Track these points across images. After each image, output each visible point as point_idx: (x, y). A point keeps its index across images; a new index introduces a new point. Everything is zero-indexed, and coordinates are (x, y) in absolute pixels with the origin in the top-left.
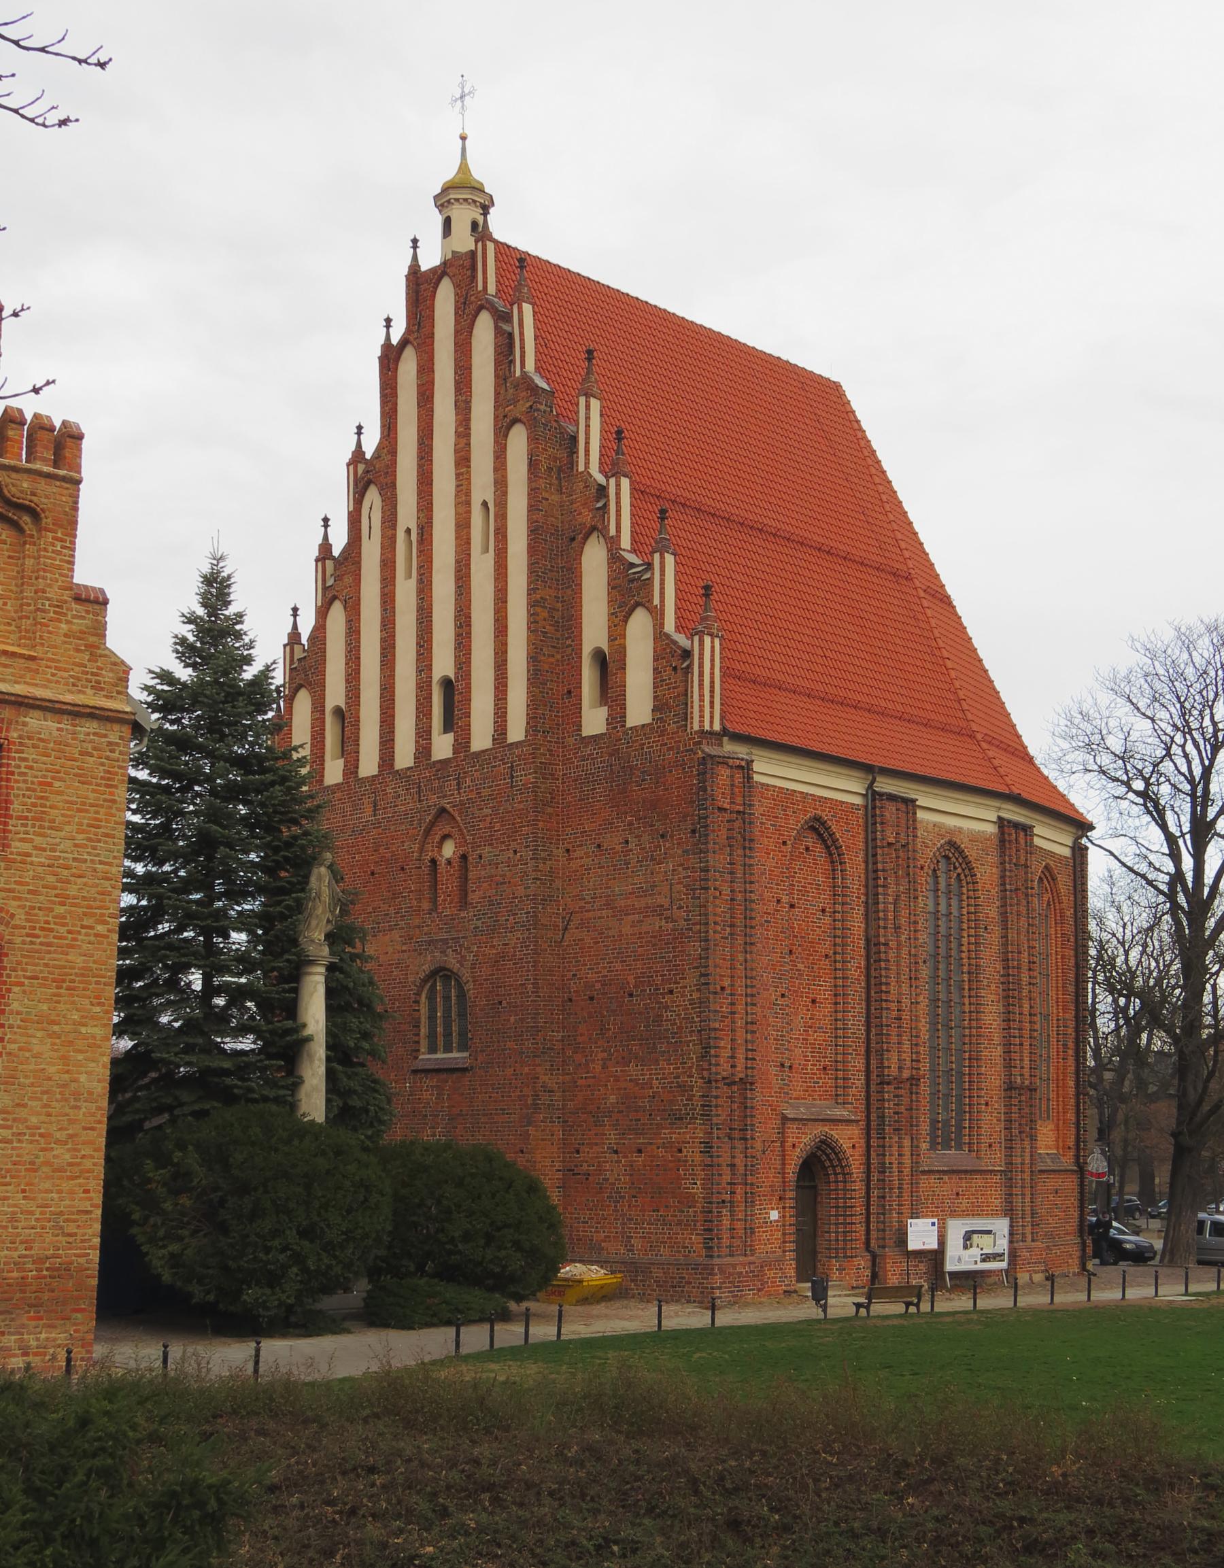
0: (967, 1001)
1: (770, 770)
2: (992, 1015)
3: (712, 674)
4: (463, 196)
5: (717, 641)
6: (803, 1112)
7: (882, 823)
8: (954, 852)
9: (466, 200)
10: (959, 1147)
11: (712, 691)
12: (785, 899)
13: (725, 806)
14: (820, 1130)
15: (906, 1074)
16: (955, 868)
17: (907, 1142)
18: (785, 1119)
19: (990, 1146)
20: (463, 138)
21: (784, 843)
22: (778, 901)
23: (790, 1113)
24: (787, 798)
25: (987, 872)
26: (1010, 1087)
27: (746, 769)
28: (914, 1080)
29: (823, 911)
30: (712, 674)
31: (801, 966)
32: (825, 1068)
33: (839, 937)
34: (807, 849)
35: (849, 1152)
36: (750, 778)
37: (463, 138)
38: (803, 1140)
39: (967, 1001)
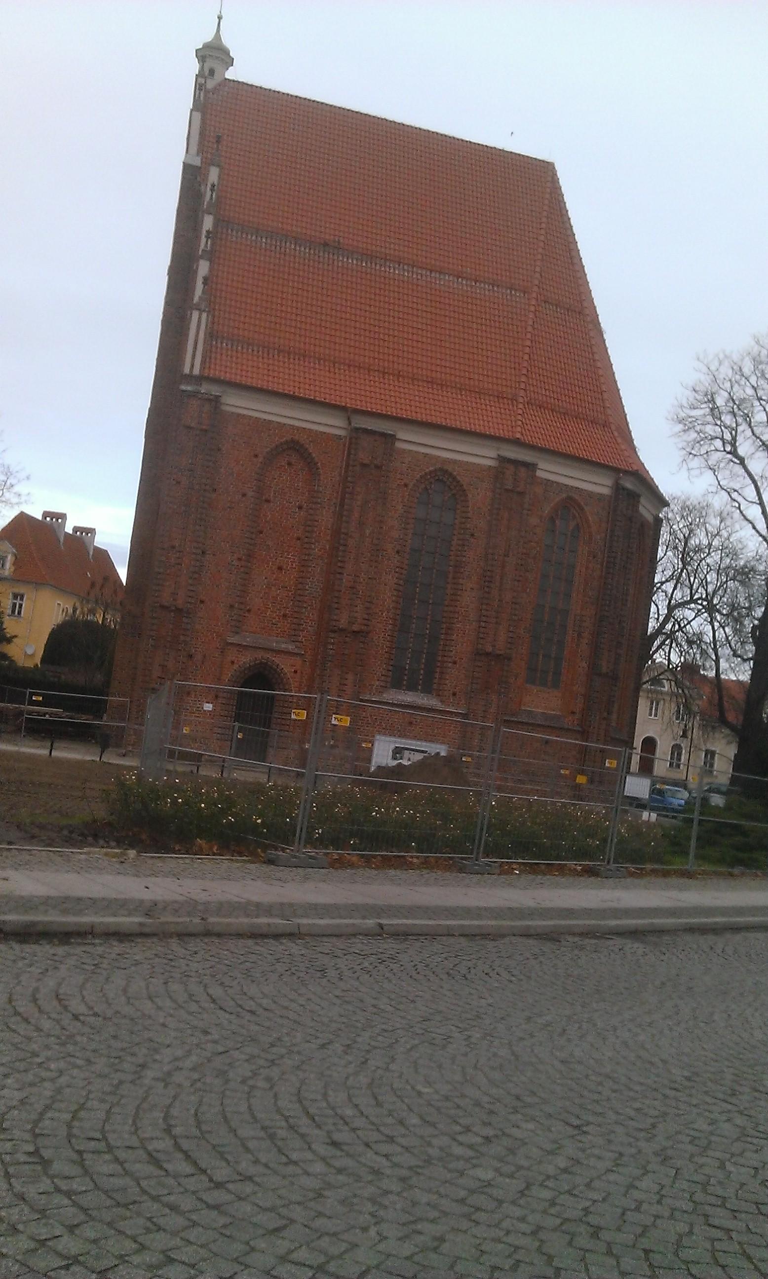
0: (449, 586)
1: (236, 403)
2: (469, 600)
4: (213, 55)
5: (204, 315)
6: (248, 640)
8: (444, 479)
9: (217, 58)
10: (427, 689)
11: (195, 348)
12: (250, 494)
14: (260, 655)
15: (355, 628)
16: (451, 490)
17: (350, 677)
19: (454, 694)
20: (220, 18)
21: (256, 456)
22: (244, 495)
24: (261, 426)
25: (480, 496)
26: (479, 654)
27: (216, 401)
29: (300, 508)
31: (270, 543)
32: (285, 616)
34: (289, 464)
35: (289, 675)
36: (216, 408)
37: (220, 18)
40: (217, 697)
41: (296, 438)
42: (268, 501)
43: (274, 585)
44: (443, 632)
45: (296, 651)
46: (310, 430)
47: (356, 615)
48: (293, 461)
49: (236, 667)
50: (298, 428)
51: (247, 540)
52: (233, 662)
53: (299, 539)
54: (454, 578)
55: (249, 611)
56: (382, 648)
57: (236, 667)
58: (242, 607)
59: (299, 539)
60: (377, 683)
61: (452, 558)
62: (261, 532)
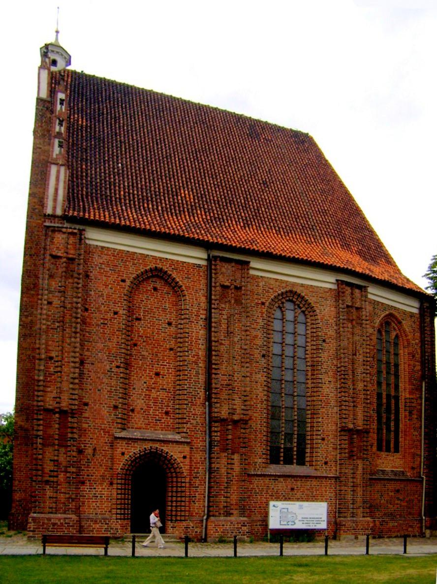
0: (309, 382)
3: (56, 190)
6: (137, 434)
7: (215, 274)
13: (59, 254)
14: (148, 446)
18: (116, 438)
23: (123, 434)
26: (344, 429)
28: (244, 422)
29: (170, 324)
30: (56, 190)
31: (147, 354)
32: (167, 413)
33: (181, 337)
34: (155, 289)
38: (135, 450)
39: (309, 382)
40: (112, 484)
41: (160, 266)
42: (138, 319)
43: (153, 388)
44: (309, 416)
45: (183, 440)
46: (172, 260)
47: (235, 407)
48: (158, 287)
49: (126, 457)
50: (161, 259)
51: (123, 351)
52: (123, 454)
53: (171, 349)
54: (312, 375)
55: (133, 411)
56: (261, 433)
57: (126, 457)
58: (126, 407)
59: (171, 349)
60: (260, 460)
61: (308, 360)
62: (135, 345)
